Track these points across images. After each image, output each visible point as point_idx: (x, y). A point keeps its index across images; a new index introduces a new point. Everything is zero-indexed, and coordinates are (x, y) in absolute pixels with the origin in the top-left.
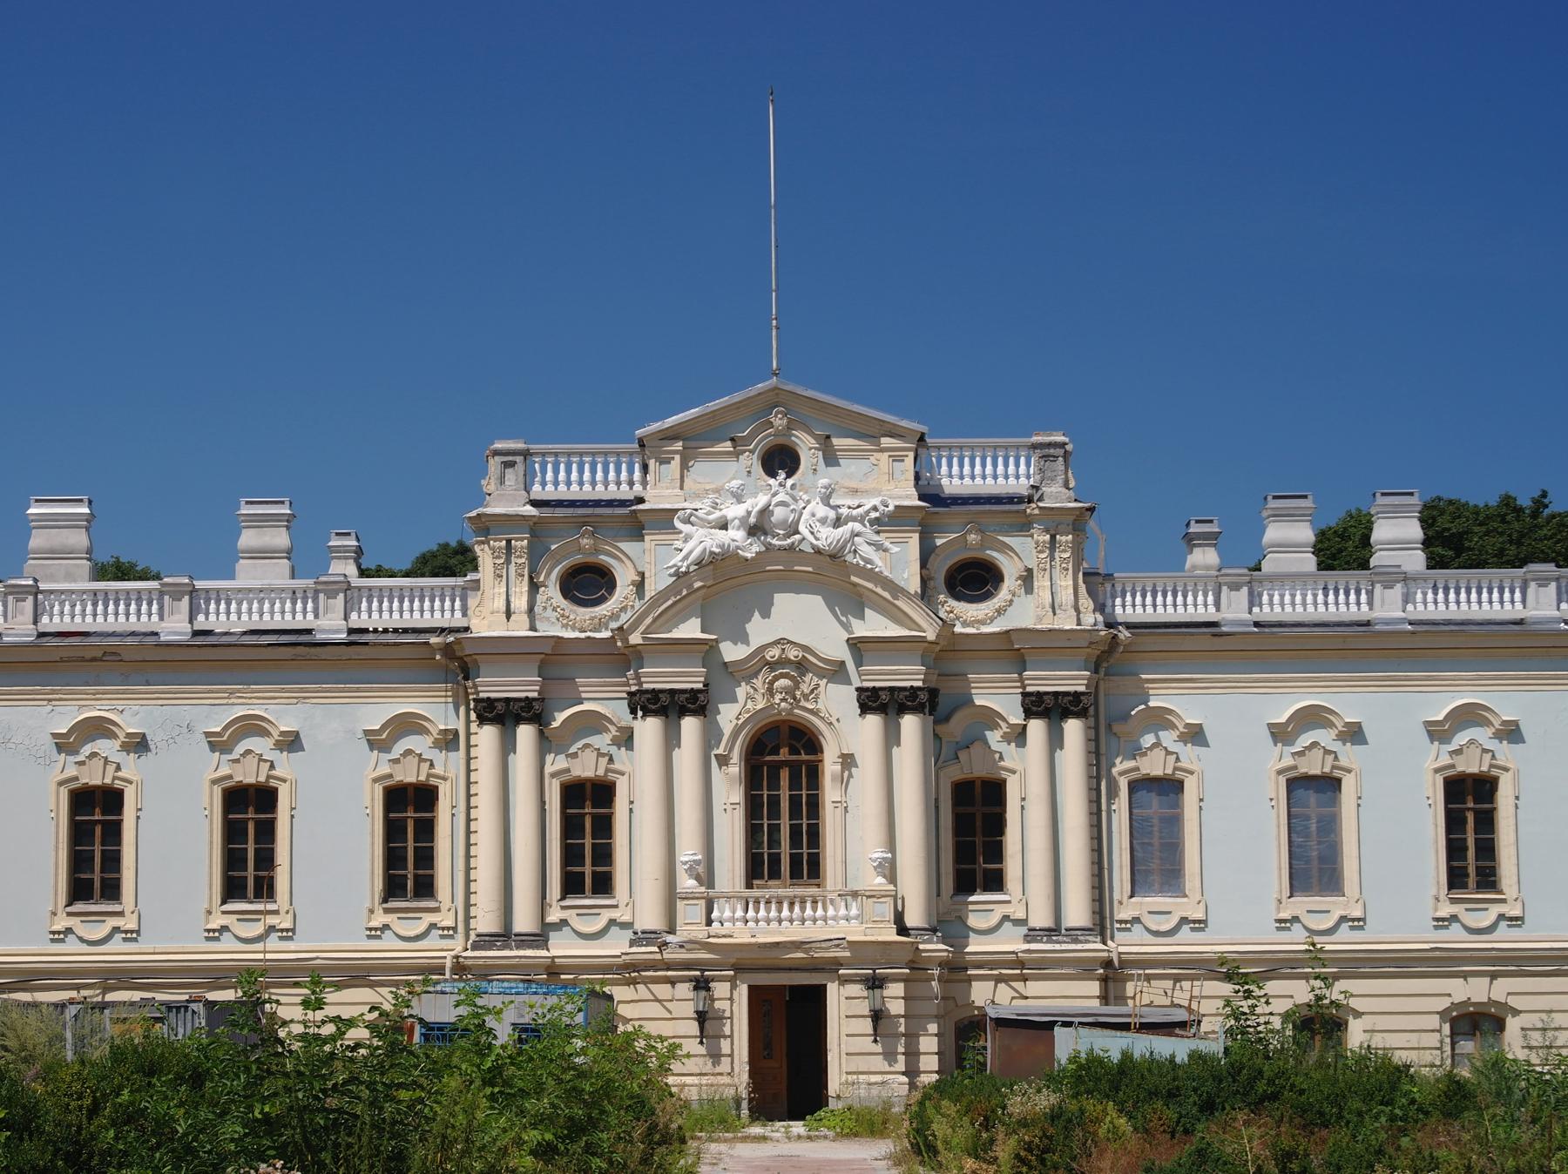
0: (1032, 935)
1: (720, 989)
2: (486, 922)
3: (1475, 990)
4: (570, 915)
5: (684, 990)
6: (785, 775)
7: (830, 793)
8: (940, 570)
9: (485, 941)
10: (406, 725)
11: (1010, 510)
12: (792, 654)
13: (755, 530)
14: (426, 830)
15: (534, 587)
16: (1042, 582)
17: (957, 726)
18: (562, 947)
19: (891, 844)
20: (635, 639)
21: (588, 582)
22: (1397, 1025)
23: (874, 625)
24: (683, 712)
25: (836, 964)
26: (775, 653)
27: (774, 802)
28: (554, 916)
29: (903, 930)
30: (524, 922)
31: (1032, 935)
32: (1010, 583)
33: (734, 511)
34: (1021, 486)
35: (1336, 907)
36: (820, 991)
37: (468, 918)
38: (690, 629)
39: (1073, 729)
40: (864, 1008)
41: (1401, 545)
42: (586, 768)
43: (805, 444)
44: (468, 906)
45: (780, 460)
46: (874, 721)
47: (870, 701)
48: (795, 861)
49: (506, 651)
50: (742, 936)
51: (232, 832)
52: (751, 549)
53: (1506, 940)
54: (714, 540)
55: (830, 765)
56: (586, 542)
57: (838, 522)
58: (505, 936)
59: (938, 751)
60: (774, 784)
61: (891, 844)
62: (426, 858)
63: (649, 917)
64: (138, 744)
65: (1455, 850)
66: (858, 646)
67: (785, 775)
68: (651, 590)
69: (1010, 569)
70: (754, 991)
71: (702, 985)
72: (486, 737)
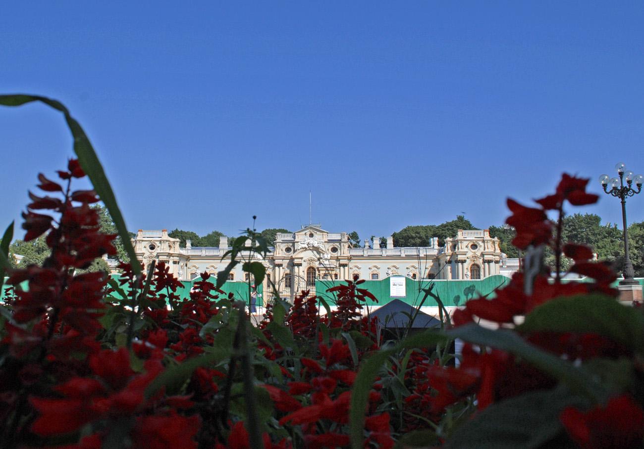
6: (311, 273)
11: (340, 241)
12: (313, 259)
13: (307, 245)
15: (282, 250)
20: (293, 257)
24: (299, 266)
27: (310, 276)
34: (340, 238)
41: (390, 244)
42: (288, 271)
45: (311, 235)
52: (307, 247)
54: (303, 246)
57: (318, 243)
60: (310, 274)
67: (311, 273)
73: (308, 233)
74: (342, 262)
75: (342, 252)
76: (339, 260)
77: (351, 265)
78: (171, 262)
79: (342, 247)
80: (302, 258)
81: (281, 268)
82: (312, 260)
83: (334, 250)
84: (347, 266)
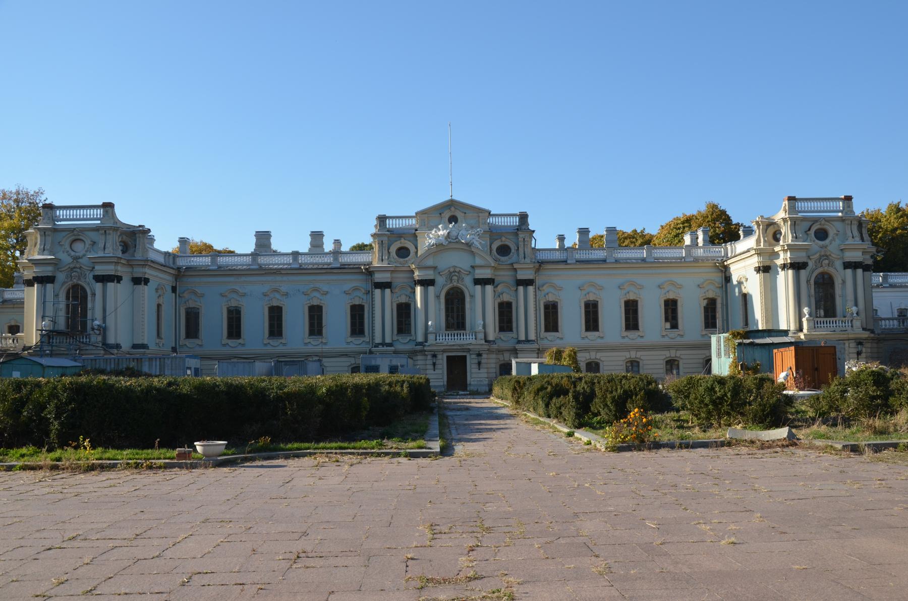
0: (519, 342)
1: (439, 357)
2: (378, 340)
3: (633, 355)
4: (400, 338)
5: (429, 357)
7: (467, 306)
8: (495, 247)
9: (377, 345)
10: (356, 289)
12: (457, 270)
14: (362, 317)
16: (521, 249)
17: (500, 288)
18: (400, 347)
19: (484, 319)
21: (403, 252)
22: (613, 365)
23: (478, 261)
25: (469, 350)
26: (452, 270)
27: (452, 308)
28: (395, 338)
29: (486, 341)
30: (388, 340)
31: (519, 342)
32: (513, 251)
33: (441, 233)
35: (596, 334)
36: (465, 356)
37: (373, 339)
38: (430, 262)
39: (531, 289)
40: (476, 361)
42: (403, 299)
43: (459, 215)
44: (373, 336)
45: (453, 219)
46: (479, 287)
47: (477, 282)
48: (458, 323)
49: (381, 270)
50: (445, 343)
51: (311, 317)
53: (639, 341)
55: (468, 299)
56: (403, 240)
58: (383, 344)
59: (496, 295)
61: (484, 319)
62: (362, 324)
63: (420, 339)
64: (286, 294)
65: (627, 319)
66: (473, 267)
68: (419, 253)
69: (513, 247)
70: (448, 357)
71: (434, 356)
72: (378, 292)
73: (447, 214)
74: (522, 275)
75: (521, 255)
76: (515, 270)
77: (538, 282)
78: (126, 280)
79: (521, 244)
80: (435, 268)
81: (388, 291)
82: (453, 273)
83: (504, 250)
84: (532, 285)
